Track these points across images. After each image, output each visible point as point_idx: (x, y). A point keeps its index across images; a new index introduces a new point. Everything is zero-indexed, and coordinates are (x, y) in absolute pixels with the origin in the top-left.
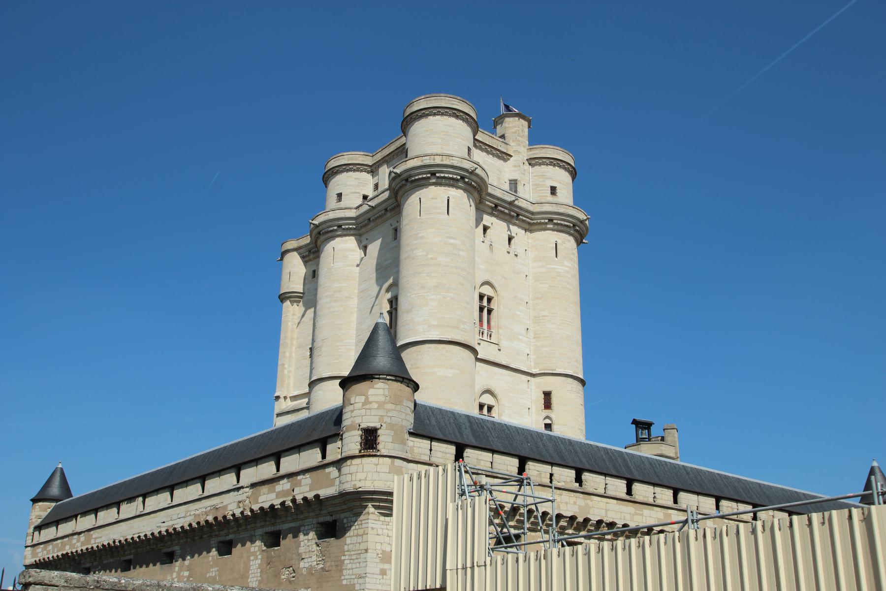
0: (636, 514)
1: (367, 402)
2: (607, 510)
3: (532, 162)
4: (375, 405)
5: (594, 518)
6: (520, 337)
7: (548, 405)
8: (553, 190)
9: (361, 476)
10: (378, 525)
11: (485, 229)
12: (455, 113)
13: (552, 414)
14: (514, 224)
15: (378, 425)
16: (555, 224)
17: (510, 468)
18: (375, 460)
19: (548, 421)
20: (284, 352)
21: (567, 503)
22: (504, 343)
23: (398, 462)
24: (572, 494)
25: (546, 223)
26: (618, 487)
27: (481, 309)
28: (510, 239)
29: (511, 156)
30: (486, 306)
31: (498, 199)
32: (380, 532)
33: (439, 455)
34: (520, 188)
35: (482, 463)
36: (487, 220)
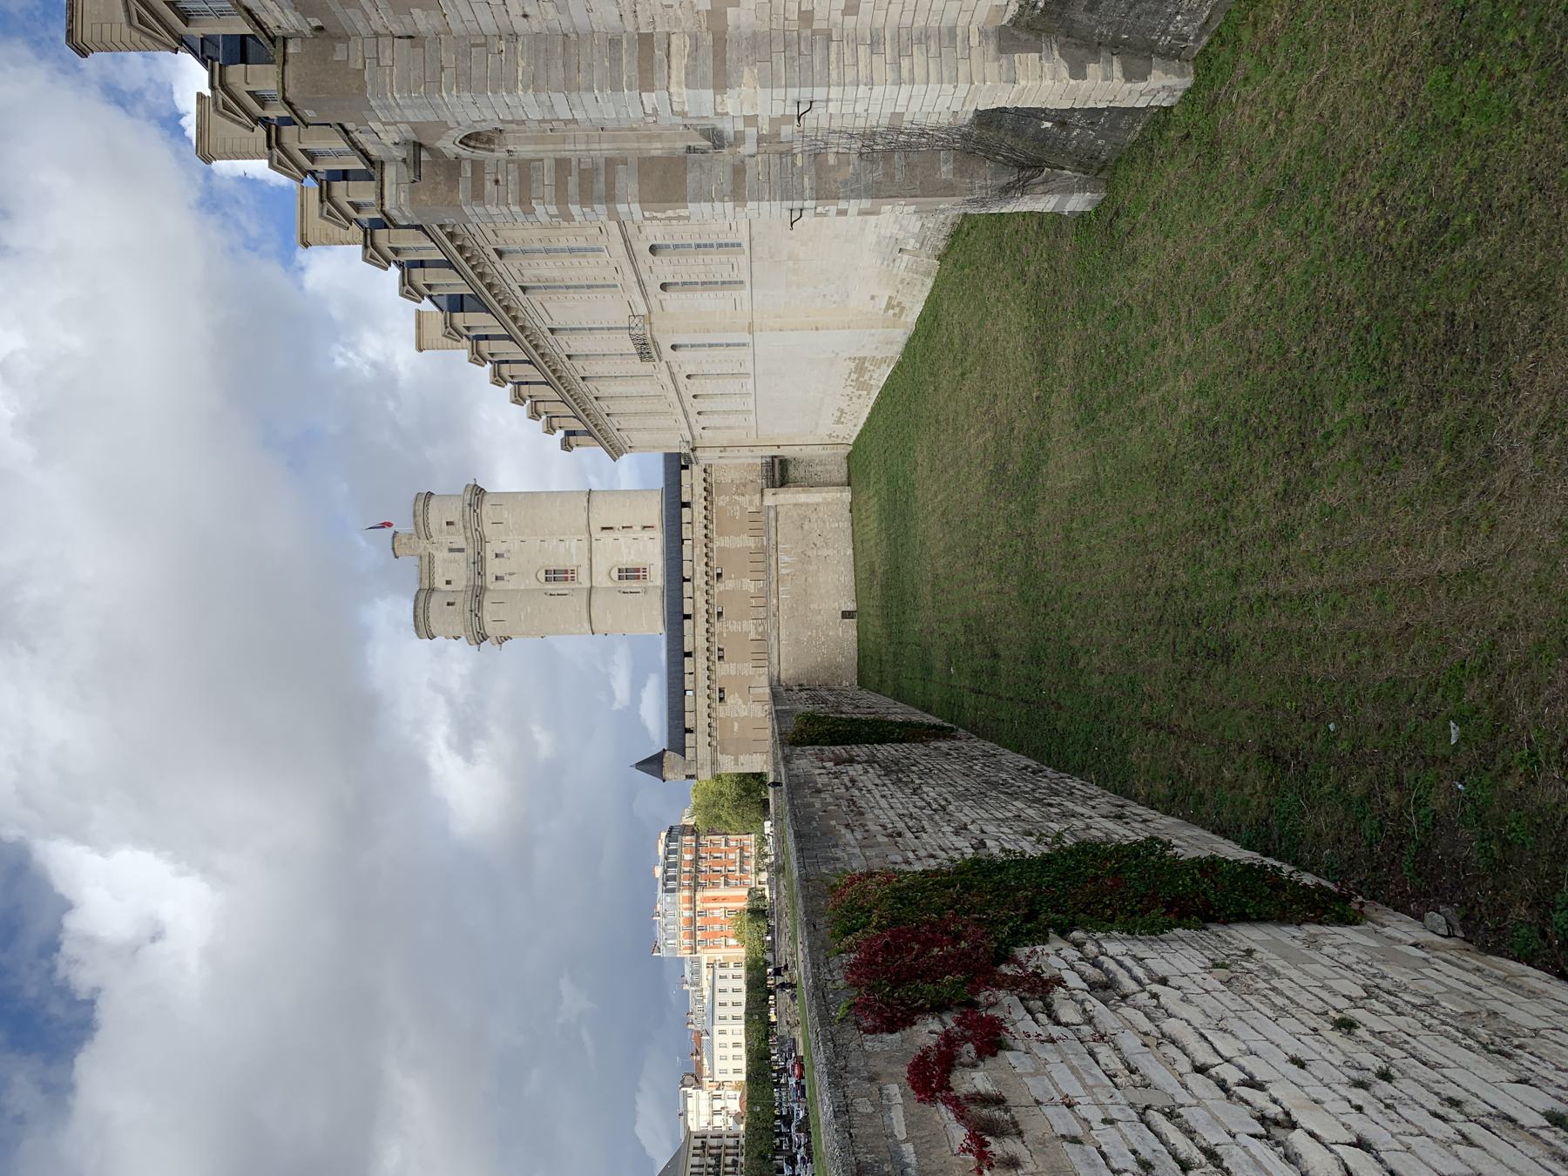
22: (575, 562)
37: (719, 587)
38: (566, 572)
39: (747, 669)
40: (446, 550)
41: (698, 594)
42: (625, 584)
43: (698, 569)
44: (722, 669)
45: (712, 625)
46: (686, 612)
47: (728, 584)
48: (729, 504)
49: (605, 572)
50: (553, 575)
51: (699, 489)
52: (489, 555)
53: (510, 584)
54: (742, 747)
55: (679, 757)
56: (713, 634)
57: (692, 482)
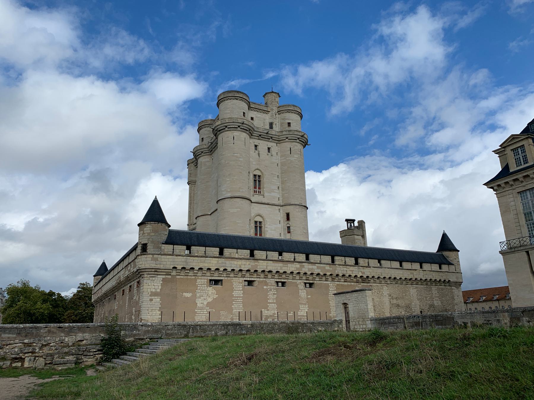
1: (144, 233)
2: (267, 266)
3: (279, 112)
4: (147, 234)
5: (260, 270)
7: (288, 219)
8: (289, 124)
9: (141, 263)
10: (149, 282)
14: (271, 142)
15: (147, 242)
17: (214, 253)
18: (145, 256)
21: (245, 265)
22: (266, 194)
23: (155, 256)
27: (255, 181)
28: (269, 149)
30: (257, 180)
31: (260, 132)
32: (150, 284)
33: (178, 251)
34: (274, 126)
36: (257, 142)
37: (300, 284)
38: (259, 188)
39: (238, 307)
40: (271, 121)
41: (298, 265)
42: (253, 225)
43: (315, 267)
44: (237, 285)
47: (303, 293)
49: (261, 212)
50: (257, 180)
51: (367, 272)
53: (253, 153)
54: (168, 299)
55: (164, 238)
56: (266, 277)
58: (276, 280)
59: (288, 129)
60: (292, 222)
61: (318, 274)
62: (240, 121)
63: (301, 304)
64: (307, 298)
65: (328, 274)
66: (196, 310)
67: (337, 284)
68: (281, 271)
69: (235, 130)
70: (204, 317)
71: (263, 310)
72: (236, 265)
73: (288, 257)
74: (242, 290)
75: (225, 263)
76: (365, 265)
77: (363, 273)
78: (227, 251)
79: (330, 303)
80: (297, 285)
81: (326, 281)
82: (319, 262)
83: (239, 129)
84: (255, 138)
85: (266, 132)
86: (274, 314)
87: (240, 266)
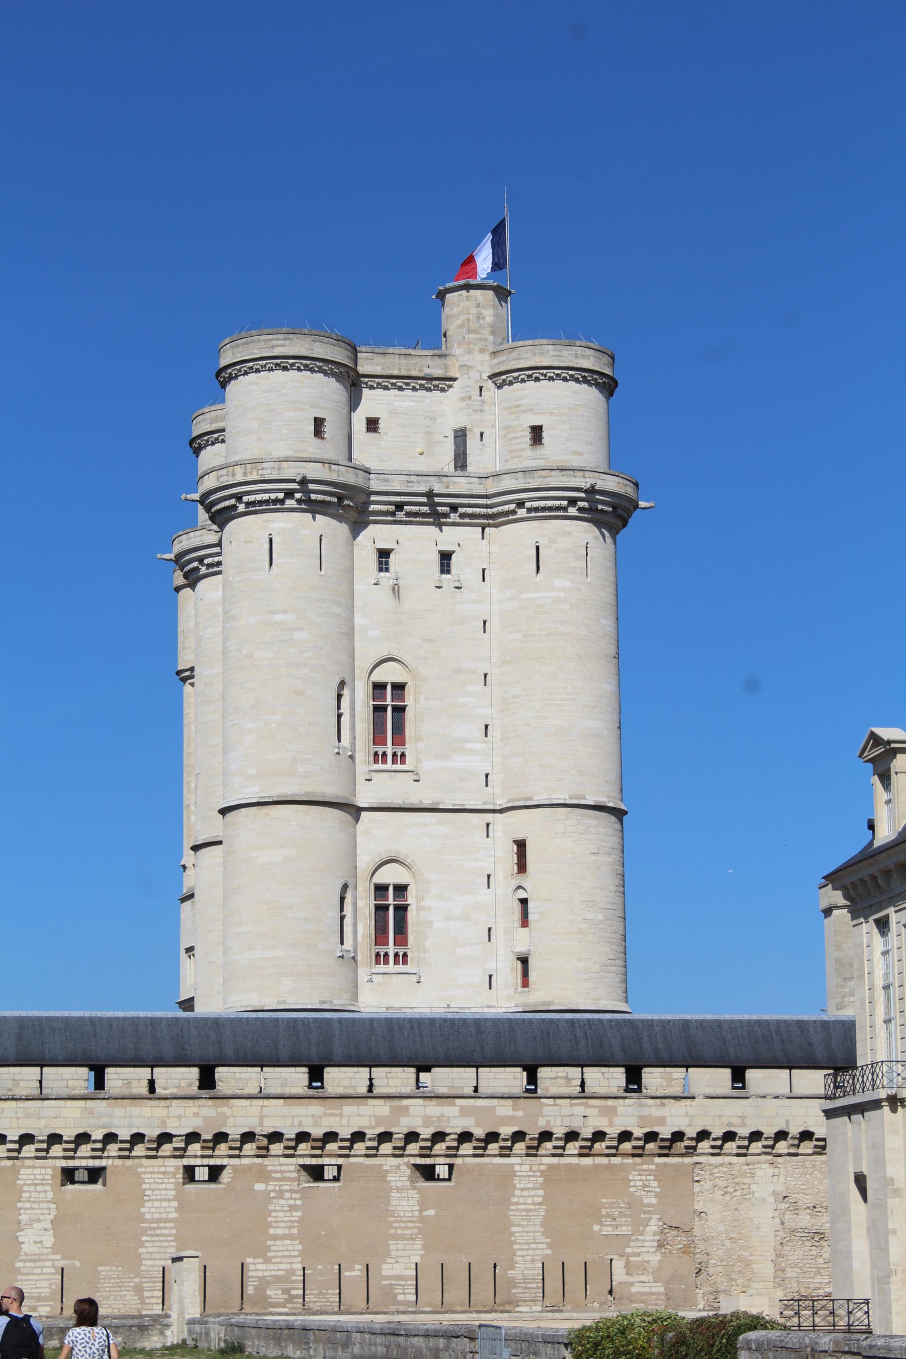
0: (326, 1115)
2: (261, 1118)
3: (500, 379)
5: (235, 1132)
6: (469, 746)
7: (522, 867)
8: (537, 433)
11: (384, 554)
12: (282, 363)
13: (527, 881)
14: (454, 524)
16: (530, 510)
17: (71, 1083)
19: (522, 894)
20: (188, 783)
21: (179, 1117)
22: (427, 766)
24: (190, 1103)
25: (514, 512)
26: (297, 1078)
27: (379, 710)
28: (446, 557)
29: (454, 379)
34: (472, 443)
35: (22, 1084)
37: (397, 1170)
41: (382, 1108)
42: (365, 902)
45: (291, 1152)
46: (331, 1074)
48: (634, 1206)
49: (399, 849)
50: (389, 710)
51: (675, 1118)
52: (451, 537)
56: (263, 1152)
57: (786, 1097)
58: (301, 1161)
59: (530, 458)
60: (535, 883)
61: (465, 1137)
62: (292, 471)
63: (397, 1237)
64: (422, 1219)
65: (506, 1131)
66: (18, 1265)
67: (551, 1167)
68: (317, 1132)
69: (277, 510)
70: (46, 1284)
71: (249, 1260)
72: (149, 1119)
73: (346, 1082)
74: (176, 1198)
75: (111, 1116)
76: (669, 1092)
77: (662, 1121)
78: (115, 1077)
79: (512, 1234)
80: (382, 1175)
81: (501, 1156)
82: (469, 1091)
83: (290, 503)
84: (376, 522)
85: (424, 489)
86: (292, 1272)
87: (163, 1123)
